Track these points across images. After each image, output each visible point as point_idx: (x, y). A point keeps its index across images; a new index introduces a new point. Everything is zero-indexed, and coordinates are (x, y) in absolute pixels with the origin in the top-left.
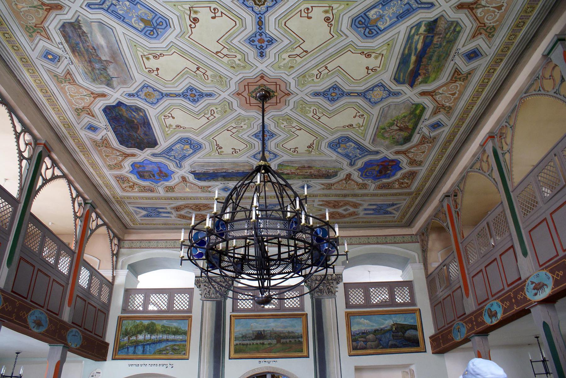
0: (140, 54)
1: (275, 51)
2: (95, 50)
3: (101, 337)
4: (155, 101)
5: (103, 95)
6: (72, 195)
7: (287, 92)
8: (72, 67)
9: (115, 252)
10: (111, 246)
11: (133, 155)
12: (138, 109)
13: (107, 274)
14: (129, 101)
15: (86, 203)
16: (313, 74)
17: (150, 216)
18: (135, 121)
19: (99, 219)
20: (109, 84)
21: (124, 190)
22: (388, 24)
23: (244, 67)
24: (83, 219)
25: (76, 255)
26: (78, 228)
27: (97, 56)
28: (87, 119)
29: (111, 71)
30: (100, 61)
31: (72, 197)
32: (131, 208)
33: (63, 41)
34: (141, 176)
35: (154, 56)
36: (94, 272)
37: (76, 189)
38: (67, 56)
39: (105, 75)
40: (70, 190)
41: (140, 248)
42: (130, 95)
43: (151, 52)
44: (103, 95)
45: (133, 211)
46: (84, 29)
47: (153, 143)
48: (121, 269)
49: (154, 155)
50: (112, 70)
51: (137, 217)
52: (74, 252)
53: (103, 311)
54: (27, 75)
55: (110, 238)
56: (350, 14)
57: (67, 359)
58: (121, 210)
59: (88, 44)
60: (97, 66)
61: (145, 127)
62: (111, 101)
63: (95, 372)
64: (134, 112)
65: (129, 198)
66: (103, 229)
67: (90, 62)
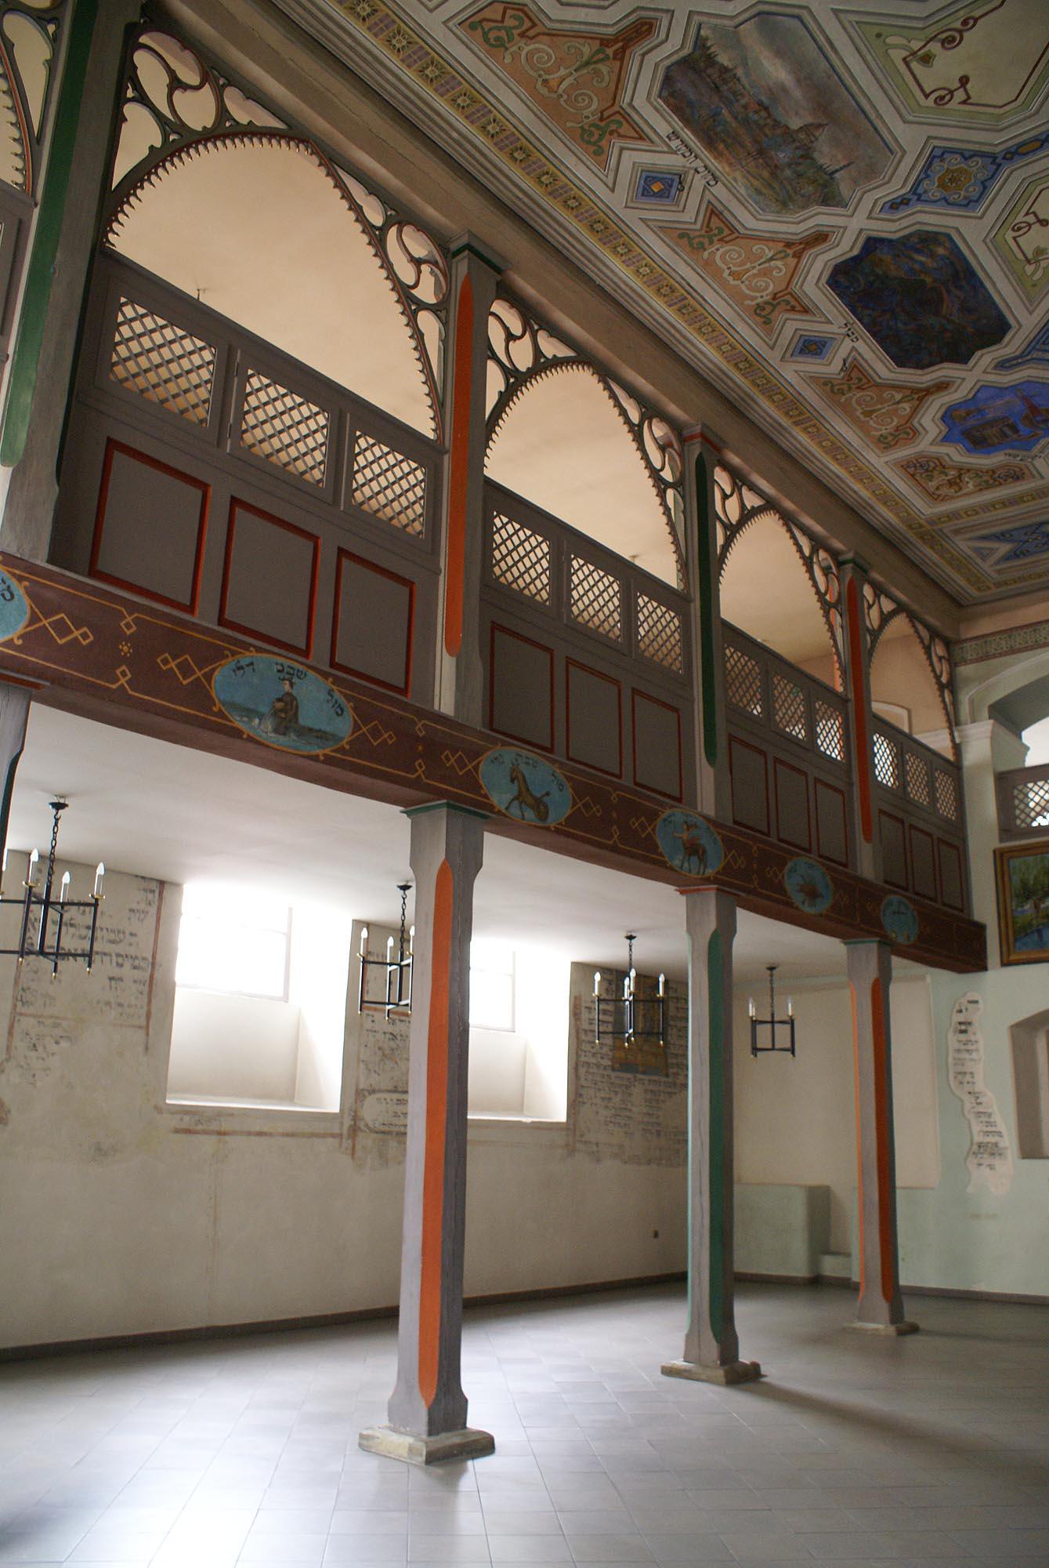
0: (897, 55)
2: (766, 109)
3: (962, 911)
4: (974, 191)
5: (819, 238)
6: (800, 550)
8: (719, 190)
9: (944, 680)
10: (931, 664)
11: (942, 386)
12: (926, 240)
13: (938, 741)
14: (894, 227)
15: (840, 564)
17: (1025, 554)
18: (928, 280)
19: (883, 598)
20: (829, 197)
21: (934, 497)
24: (844, 606)
25: (851, 706)
26: (839, 632)
27: (777, 124)
28: (791, 327)
29: (826, 154)
30: (788, 135)
31: (803, 556)
32: (964, 545)
33: (678, 125)
34: (977, 441)
35: (943, 42)
36: (904, 744)
37: (805, 531)
38: (698, 164)
39: (810, 173)
40: (793, 537)
41: (1013, 651)
42: (895, 205)
43: (931, 32)
44: (819, 238)
45: (970, 552)
46: (723, 59)
47: (996, 328)
48: (973, 721)
49: (1003, 365)
50: (826, 149)
51: (987, 567)
52: (845, 701)
53: (952, 839)
54: (616, 264)
55: (922, 642)
57: (894, 974)
58: (935, 557)
59: (743, 102)
60: (782, 156)
61: (961, 288)
62: (846, 247)
63: (964, 1001)
64: (918, 251)
65: (955, 515)
66: (900, 624)
67: (761, 152)
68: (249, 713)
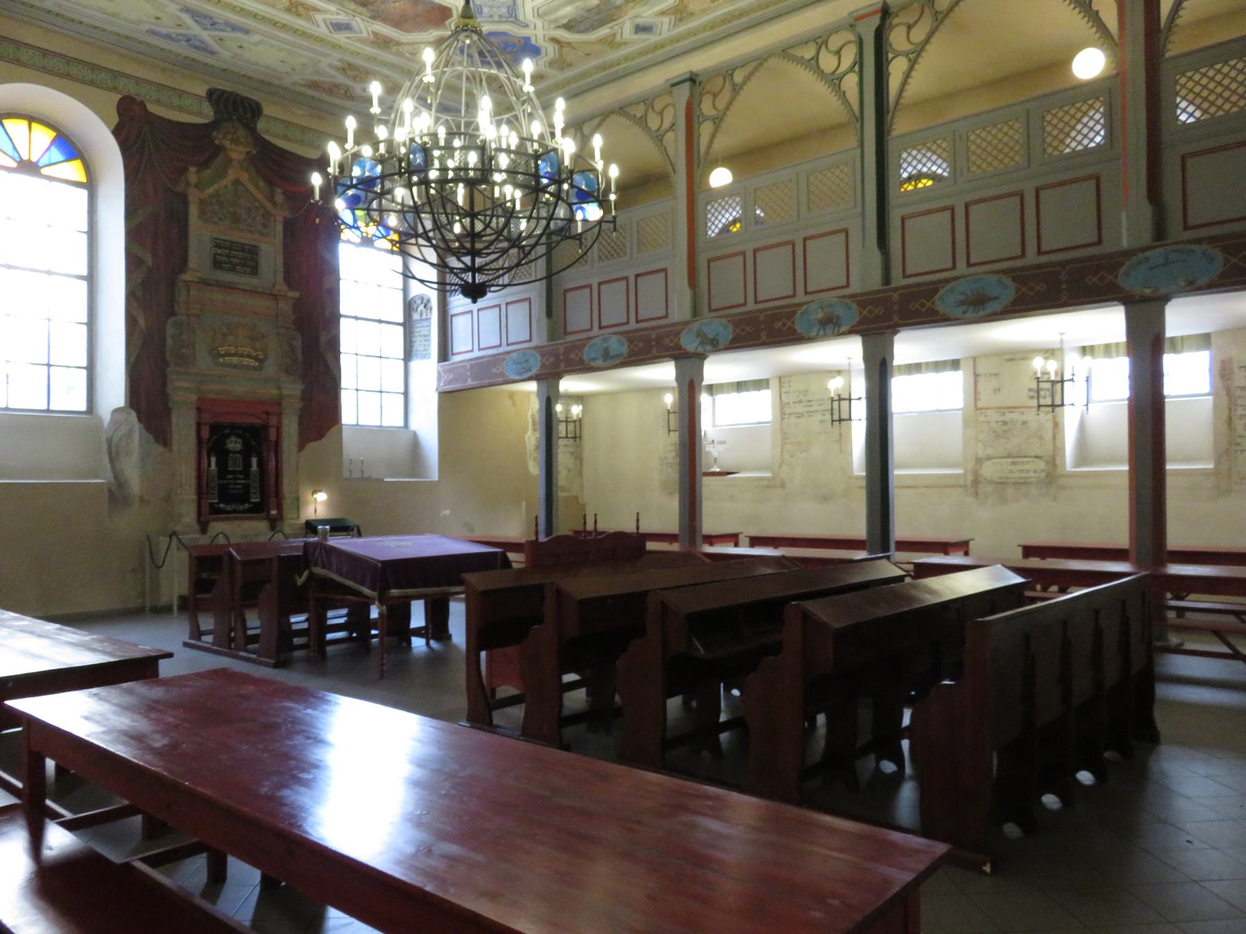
68: (595, 359)
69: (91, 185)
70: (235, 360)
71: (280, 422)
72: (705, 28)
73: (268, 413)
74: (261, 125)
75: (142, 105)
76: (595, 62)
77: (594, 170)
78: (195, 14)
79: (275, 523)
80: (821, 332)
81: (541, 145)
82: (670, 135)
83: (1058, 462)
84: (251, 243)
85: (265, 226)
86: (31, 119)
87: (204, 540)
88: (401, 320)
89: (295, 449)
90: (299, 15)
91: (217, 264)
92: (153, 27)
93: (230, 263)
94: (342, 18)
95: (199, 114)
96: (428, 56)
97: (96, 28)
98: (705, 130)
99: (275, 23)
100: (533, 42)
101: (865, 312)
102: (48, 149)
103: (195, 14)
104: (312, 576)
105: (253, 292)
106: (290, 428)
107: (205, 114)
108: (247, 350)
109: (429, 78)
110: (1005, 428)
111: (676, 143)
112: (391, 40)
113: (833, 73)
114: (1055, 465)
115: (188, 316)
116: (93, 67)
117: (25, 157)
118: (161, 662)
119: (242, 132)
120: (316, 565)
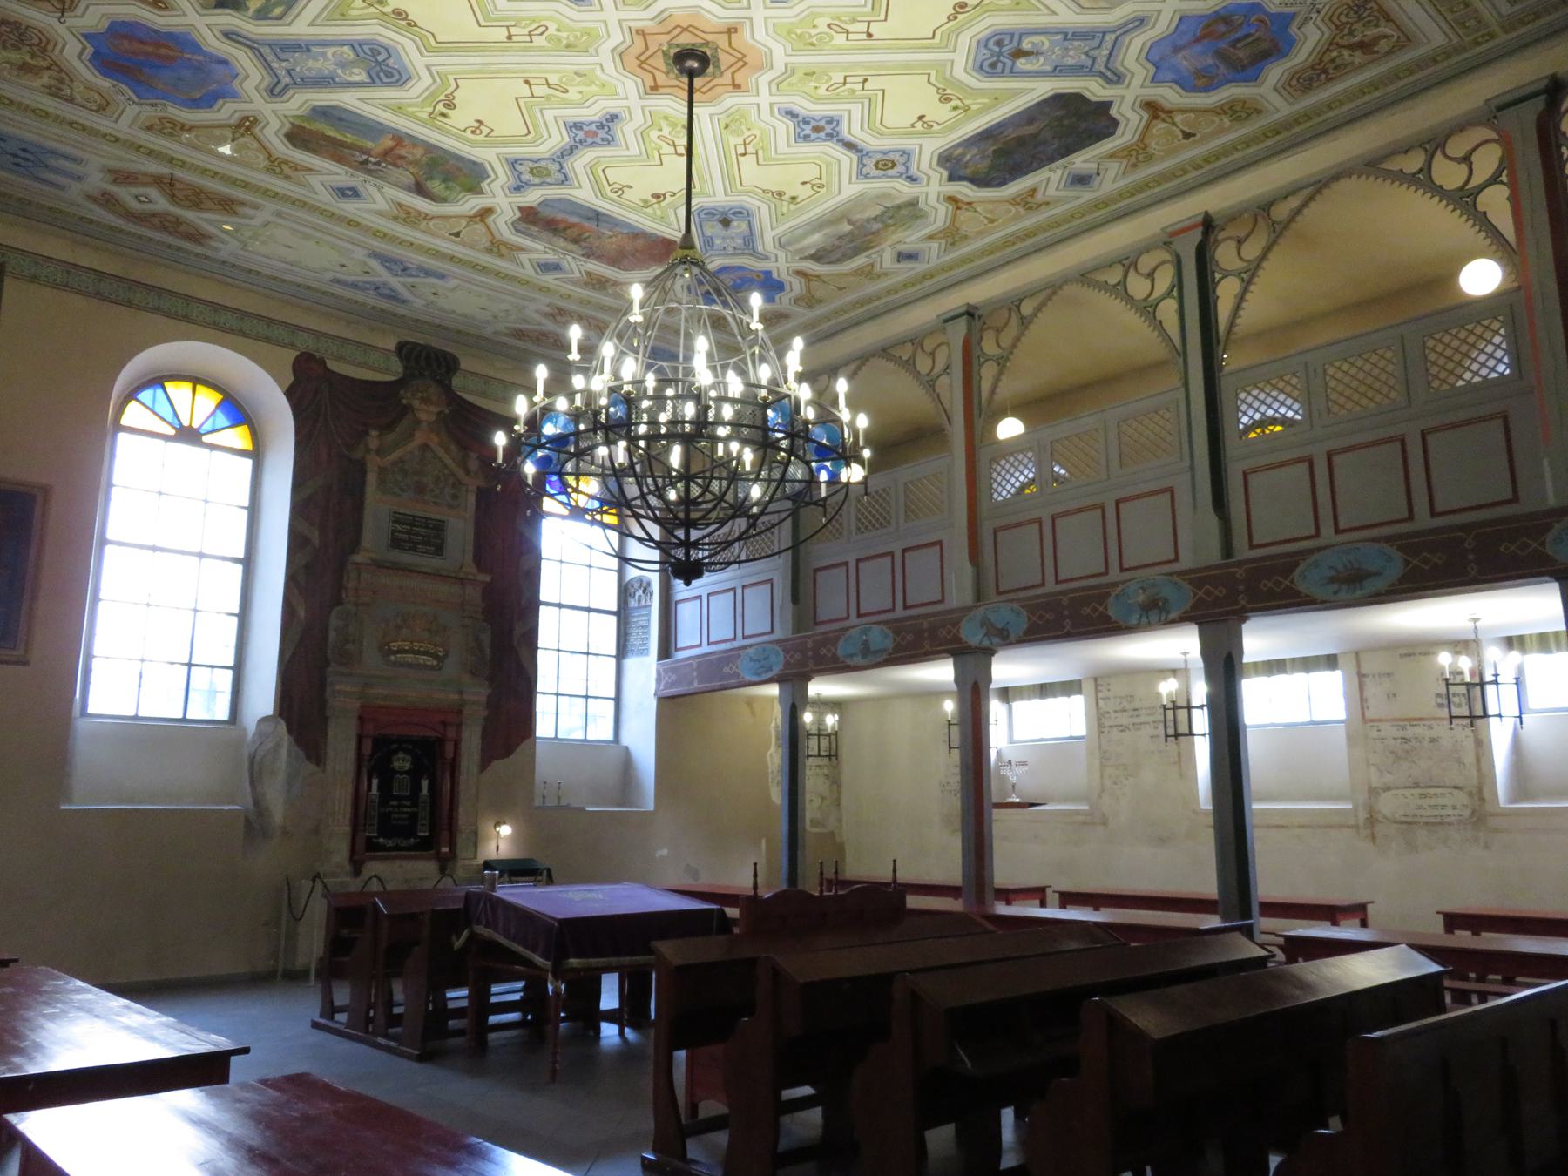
1: (585, 112)
7: (639, 40)
16: (549, 39)
22: (333, 49)
23: (666, 118)
56: (403, 94)
68: (852, 656)
69: (257, 455)
70: (409, 658)
71: (459, 732)
72: (983, 253)
73: (444, 724)
74: (457, 382)
75: (322, 362)
76: (850, 297)
77: (837, 421)
78: (385, 260)
79: (446, 864)
80: (1144, 620)
81: (770, 392)
82: (944, 380)
83: (1486, 795)
84: (439, 517)
85: (455, 497)
86: (196, 380)
87: (354, 885)
88: (614, 608)
89: (475, 769)
90: (502, 256)
91: (396, 543)
92: (338, 276)
93: (410, 541)
94: (551, 257)
95: (387, 371)
96: (637, 292)
97: (275, 279)
98: (987, 373)
99: (474, 266)
100: (775, 276)
101: (1200, 594)
102: (213, 413)
103: (385, 260)
104: (473, 937)
105: (437, 575)
106: (471, 741)
107: (393, 370)
108: (425, 646)
109: (636, 317)
110: (1406, 746)
111: (951, 389)
112: (608, 280)
113: (1145, 300)
114: (1482, 800)
115: (357, 605)
116: (270, 322)
117: (186, 424)
118: (234, 1060)
119: (434, 391)
120: (479, 922)
